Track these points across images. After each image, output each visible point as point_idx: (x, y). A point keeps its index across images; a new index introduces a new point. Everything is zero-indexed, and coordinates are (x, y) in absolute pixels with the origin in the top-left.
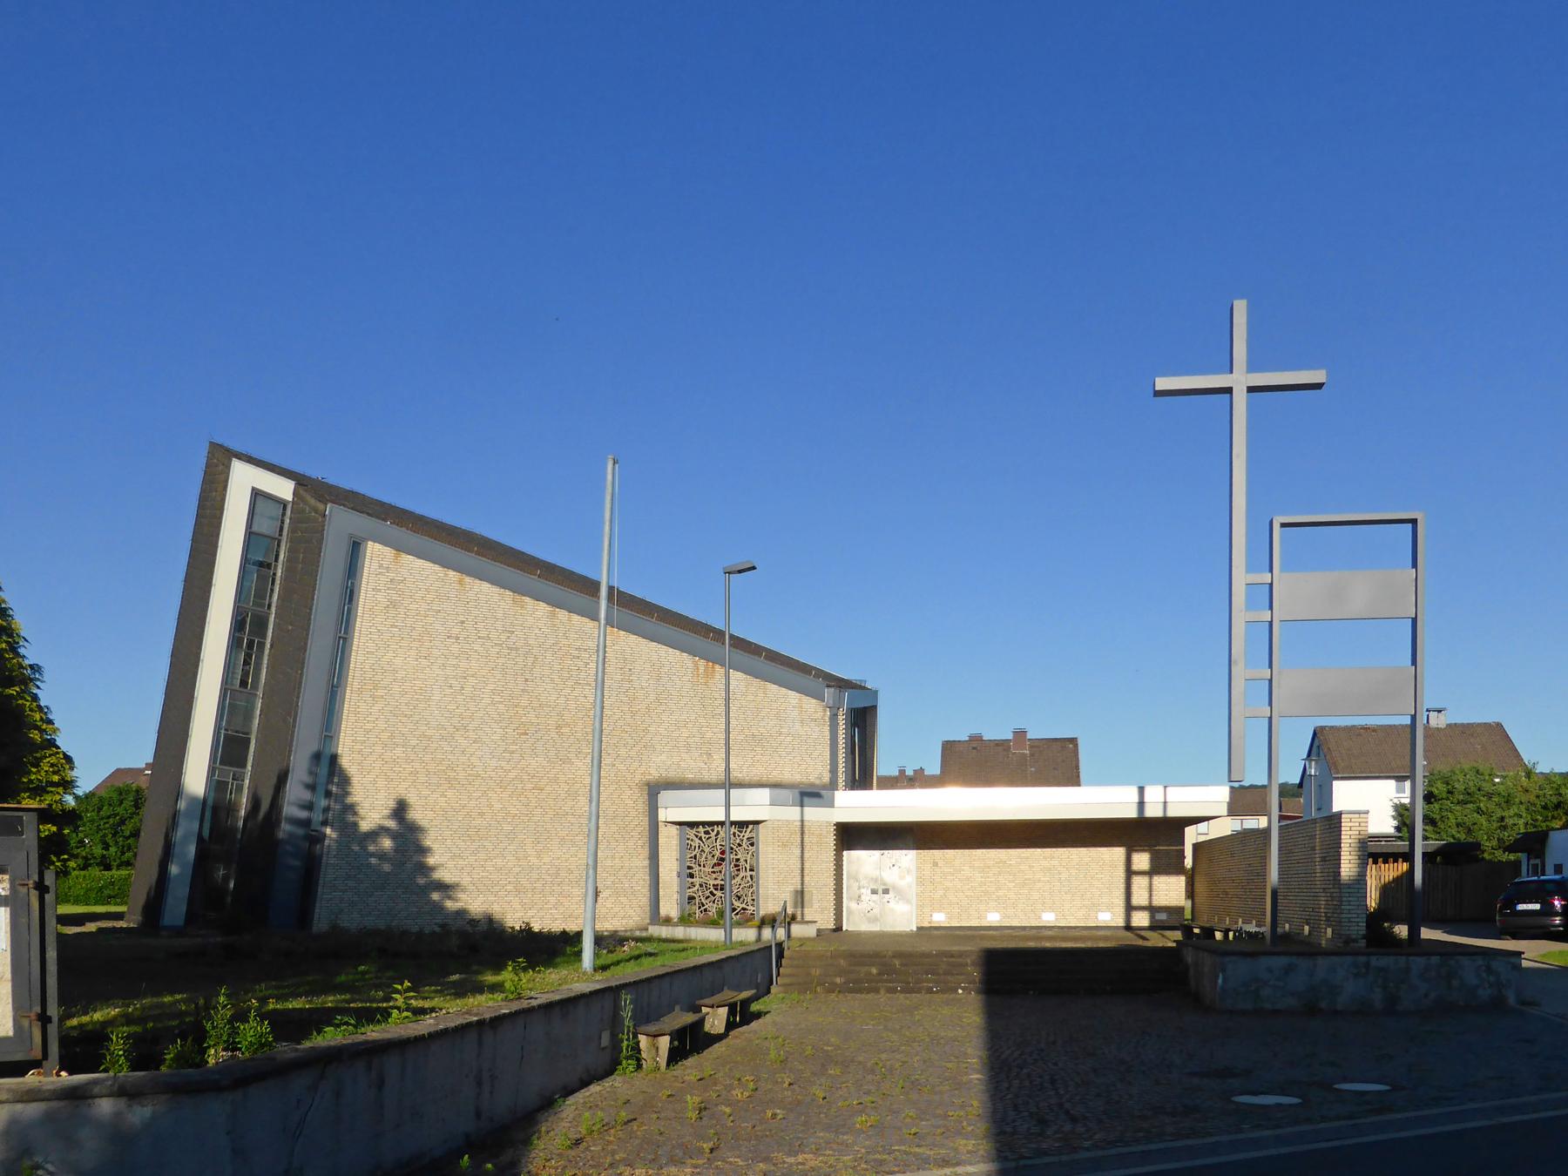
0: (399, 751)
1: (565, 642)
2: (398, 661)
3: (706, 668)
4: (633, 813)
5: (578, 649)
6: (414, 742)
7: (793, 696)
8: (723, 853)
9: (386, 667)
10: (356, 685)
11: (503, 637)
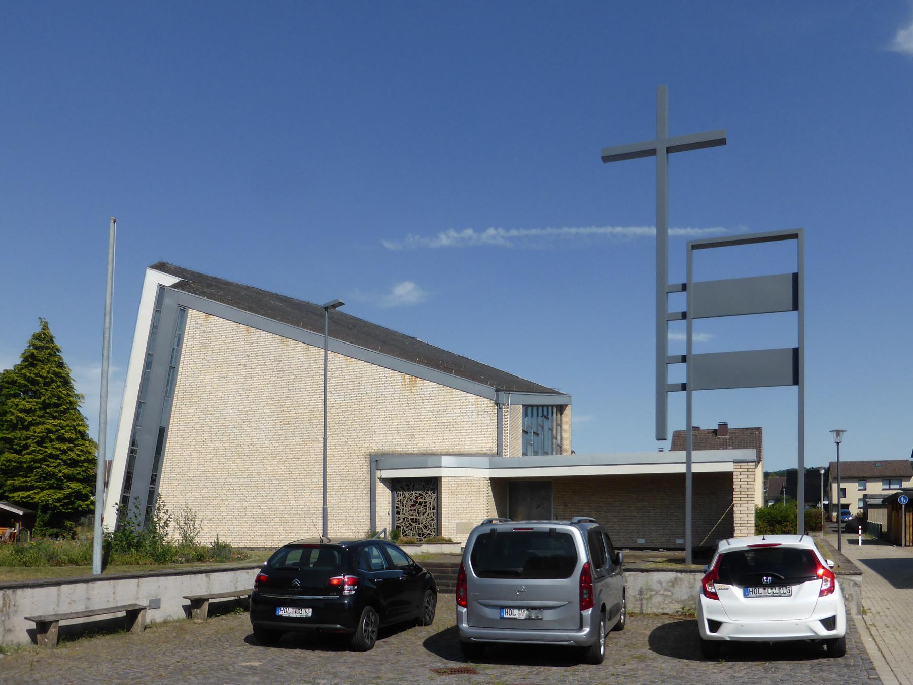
0: (206, 436)
1: (314, 366)
2: (207, 380)
3: (411, 380)
4: (360, 473)
6: (216, 430)
7: (472, 398)
8: (416, 498)
9: (199, 384)
10: (180, 396)
11: (275, 364)
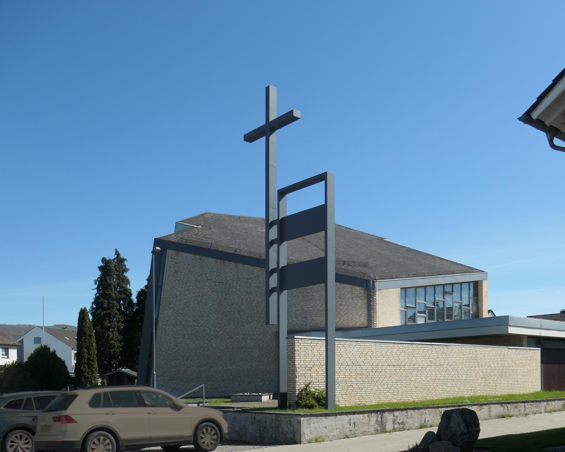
5: (247, 279)
